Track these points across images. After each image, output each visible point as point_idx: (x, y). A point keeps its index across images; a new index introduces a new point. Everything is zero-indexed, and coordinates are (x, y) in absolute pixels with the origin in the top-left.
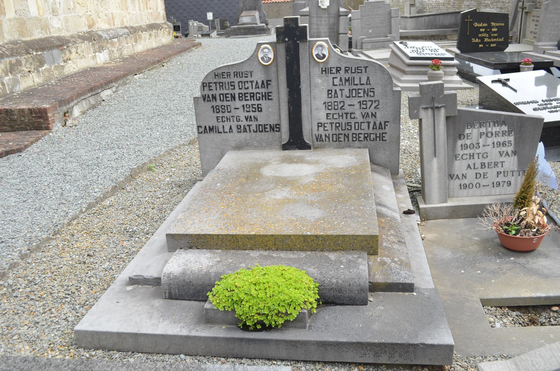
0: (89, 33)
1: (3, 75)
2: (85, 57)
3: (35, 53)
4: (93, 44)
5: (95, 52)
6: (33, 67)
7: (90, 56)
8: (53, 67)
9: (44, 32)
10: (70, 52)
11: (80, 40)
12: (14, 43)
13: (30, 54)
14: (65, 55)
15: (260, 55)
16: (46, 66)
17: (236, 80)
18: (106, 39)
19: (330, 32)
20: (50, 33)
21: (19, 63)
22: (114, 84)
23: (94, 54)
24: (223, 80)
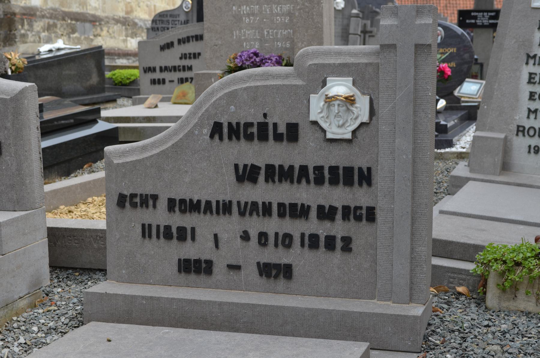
0: (125, 18)
1: (41, 31)
2: (115, 38)
3: (69, 21)
4: (126, 29)
5: (127, 36)
6: (65, 32)
7: (121, 38)
8: (83, 37)
9: (81, 7)
10: (102, 30)
11: (113, 22)
12: (55, 10)
13: (65, 21)
14: (96, 29)
15: (184, 5)
16: (76, 35)
17: (171, 19)
18: (141, 27)
19: (342, 32)
20: (87, 9)
21: (55, 25)
22: (132, 58)
23: (125, 38)
24: (164, 19)
